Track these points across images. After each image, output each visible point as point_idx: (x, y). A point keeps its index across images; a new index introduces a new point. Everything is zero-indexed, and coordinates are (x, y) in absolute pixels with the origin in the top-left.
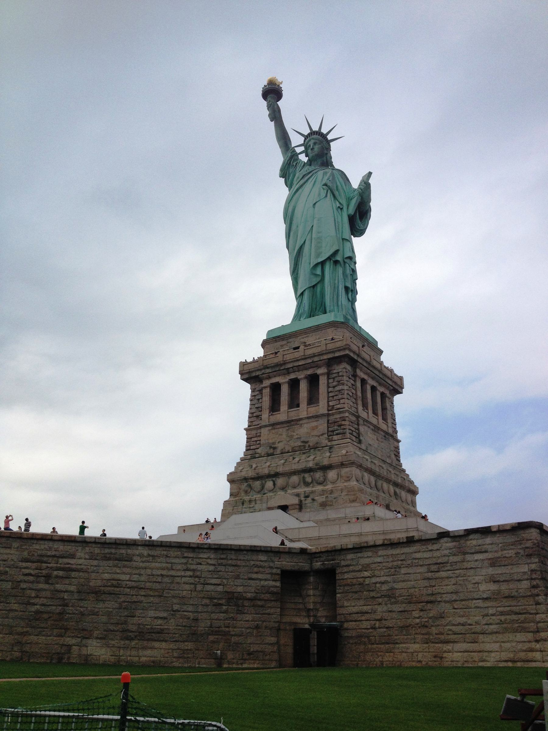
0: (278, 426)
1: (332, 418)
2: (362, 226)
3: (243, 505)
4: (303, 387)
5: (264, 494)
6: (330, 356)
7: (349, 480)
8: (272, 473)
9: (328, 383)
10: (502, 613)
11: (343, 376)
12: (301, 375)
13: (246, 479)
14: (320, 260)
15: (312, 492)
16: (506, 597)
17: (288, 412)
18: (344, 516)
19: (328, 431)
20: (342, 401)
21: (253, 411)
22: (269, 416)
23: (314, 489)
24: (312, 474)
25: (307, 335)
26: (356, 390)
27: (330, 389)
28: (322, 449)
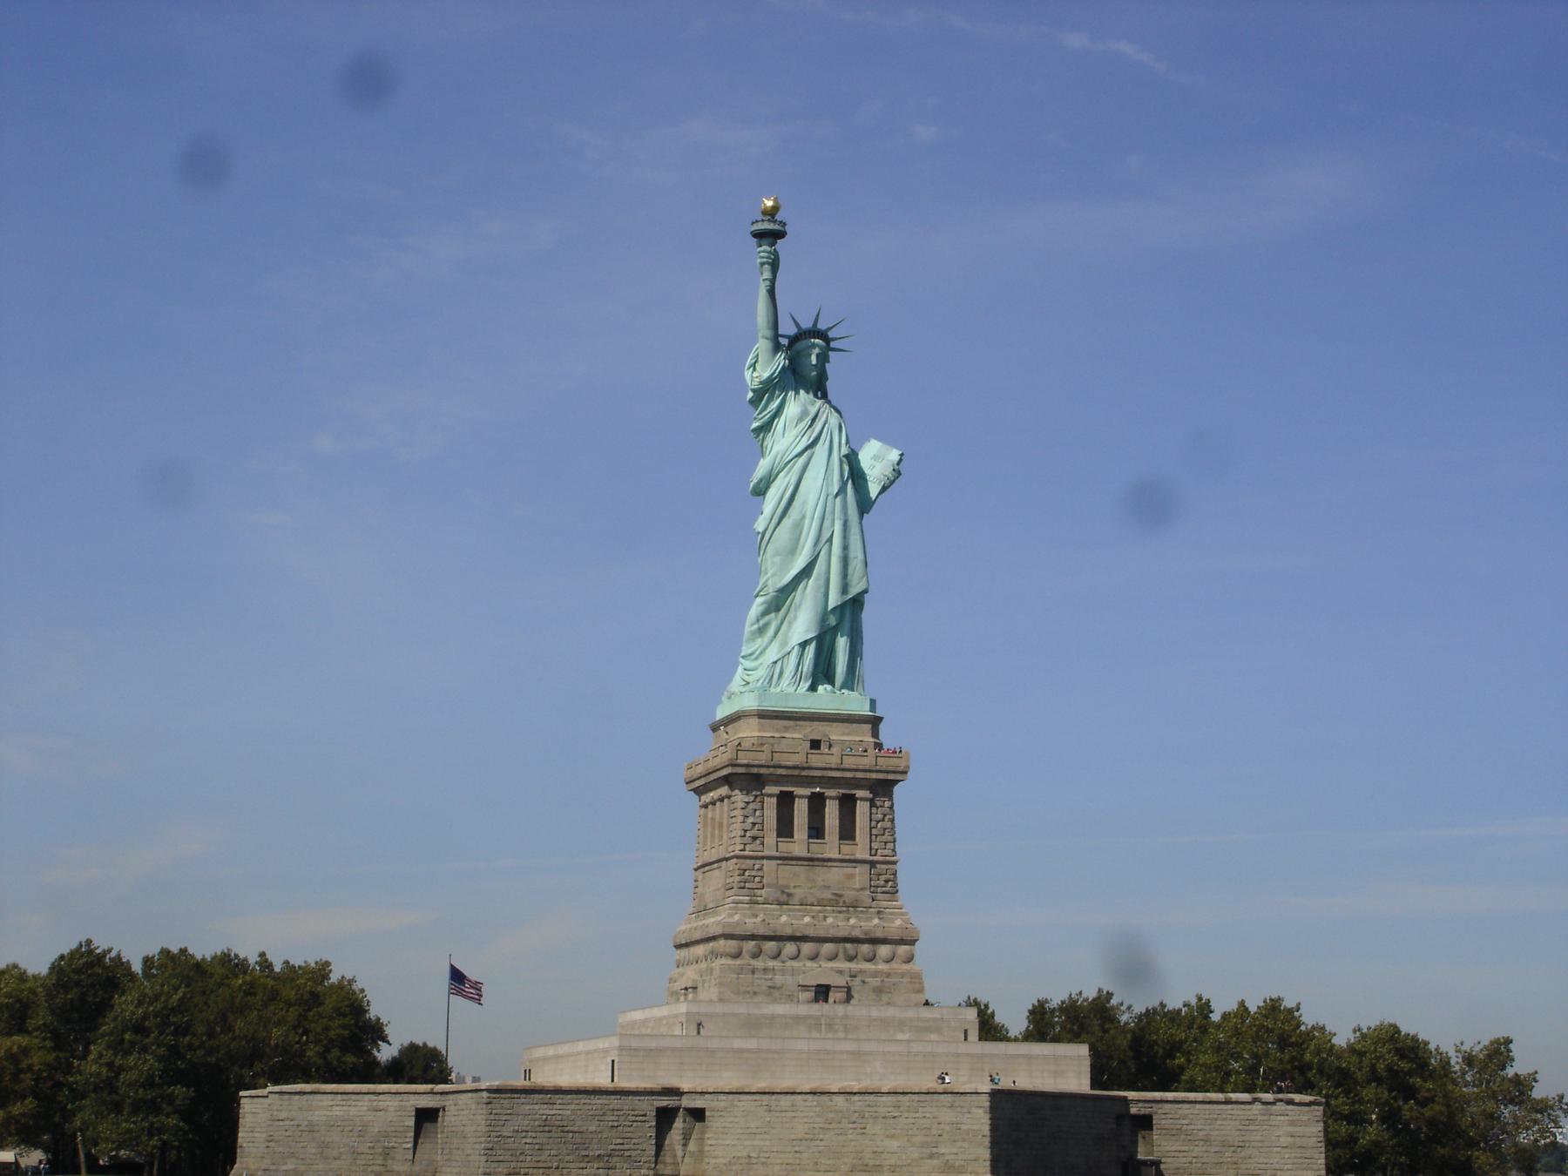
0: (794, 862)
4: (832, 811)
6: (881, 776)
7: (909, 962)
8: (798, 934)
9: (871, 814)
10: (1295, 1158)
13: (753, 937)
15: (862, 971)
16: (1299, 1147)
17: (809, 843)
18: (939, 1017)
19: (871, 886)
22: (777, 842)
23: (860, 966)
24: (856, 945)
27: (873, 823)
28: (867, 911)
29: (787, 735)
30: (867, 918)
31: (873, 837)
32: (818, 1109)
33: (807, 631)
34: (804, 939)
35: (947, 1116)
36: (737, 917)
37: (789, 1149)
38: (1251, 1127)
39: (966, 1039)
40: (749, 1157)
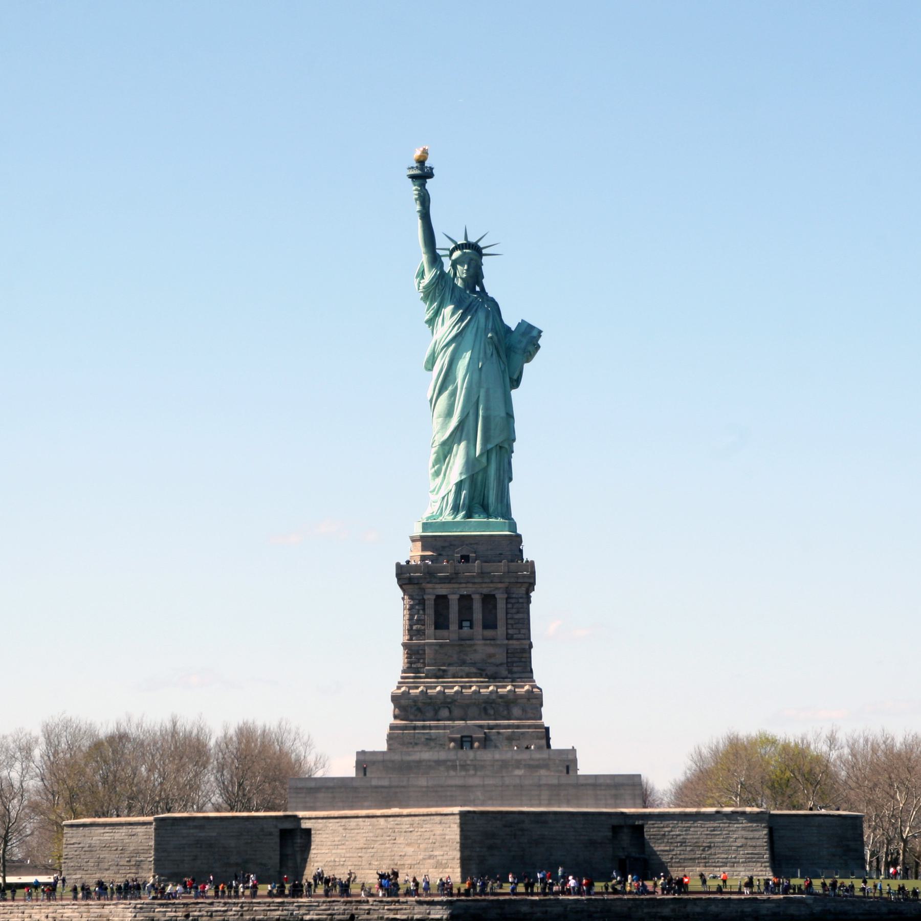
4: (477, 606)
6: (513, 580)
9: (507, 608)
10: (748, 854)
14: (489, 446)
19: (507, 662)
24: (493, 705)
27: (509, 616)
29: (442, 552)
31: (510, 626)
32: (371, 827)
33: (461, 474)
35: (438, 830)
36: (403, 689)
37: (355, 855)
38: (715, 832)
40: (335, 861)
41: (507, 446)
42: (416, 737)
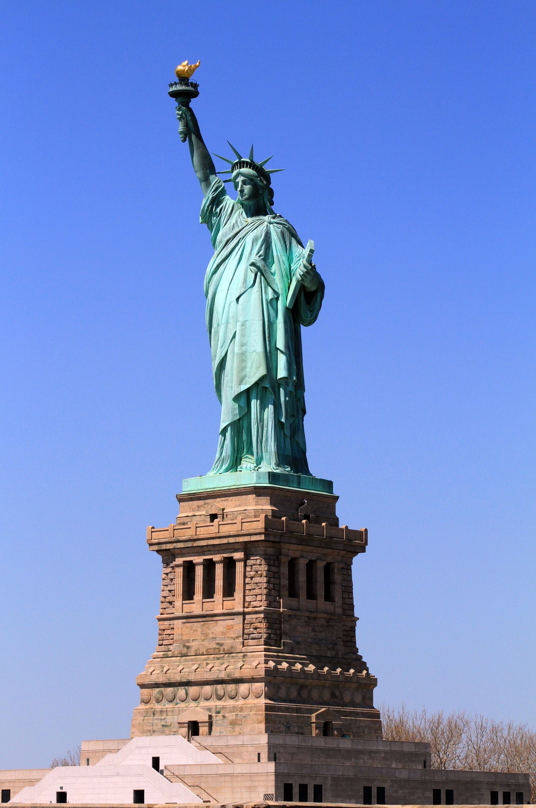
1: (247, 617)
2: (309, 314)
3: (154, 716)
5: (177, 704)
6: (246, 539)
7: (260, 697)
11: (260, 565)
12: (216, 558)
13: (157, 685)
14: (244, 387)
15: (224, 708)
17: (203, 602)
19: (243, 633)
20: (259, 597)
21: (166, 593)
22: (183, 604)
23: (225, 704)
24: (224, 685)
25: (226, 498)
26: (279, 578)
27: (247, 580)
30: (235, 661)
33: (223, 421)
34: (188, 684)
39: (259, 761)
41: (268, 386)
42: (154, 724)
